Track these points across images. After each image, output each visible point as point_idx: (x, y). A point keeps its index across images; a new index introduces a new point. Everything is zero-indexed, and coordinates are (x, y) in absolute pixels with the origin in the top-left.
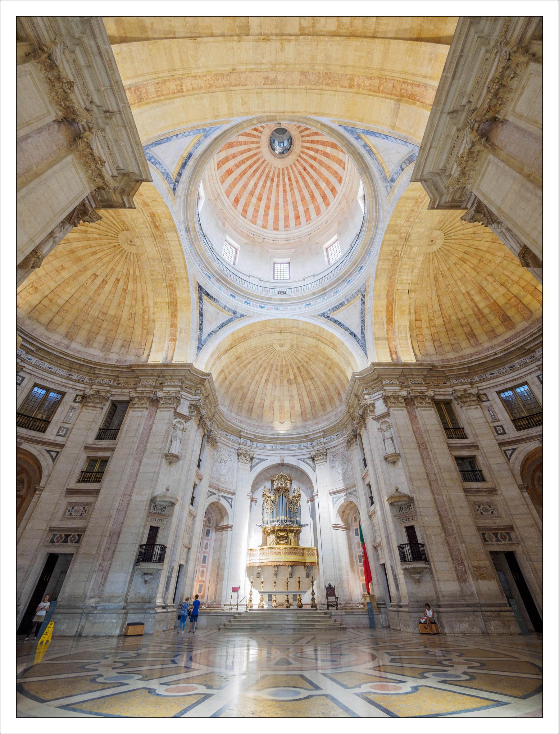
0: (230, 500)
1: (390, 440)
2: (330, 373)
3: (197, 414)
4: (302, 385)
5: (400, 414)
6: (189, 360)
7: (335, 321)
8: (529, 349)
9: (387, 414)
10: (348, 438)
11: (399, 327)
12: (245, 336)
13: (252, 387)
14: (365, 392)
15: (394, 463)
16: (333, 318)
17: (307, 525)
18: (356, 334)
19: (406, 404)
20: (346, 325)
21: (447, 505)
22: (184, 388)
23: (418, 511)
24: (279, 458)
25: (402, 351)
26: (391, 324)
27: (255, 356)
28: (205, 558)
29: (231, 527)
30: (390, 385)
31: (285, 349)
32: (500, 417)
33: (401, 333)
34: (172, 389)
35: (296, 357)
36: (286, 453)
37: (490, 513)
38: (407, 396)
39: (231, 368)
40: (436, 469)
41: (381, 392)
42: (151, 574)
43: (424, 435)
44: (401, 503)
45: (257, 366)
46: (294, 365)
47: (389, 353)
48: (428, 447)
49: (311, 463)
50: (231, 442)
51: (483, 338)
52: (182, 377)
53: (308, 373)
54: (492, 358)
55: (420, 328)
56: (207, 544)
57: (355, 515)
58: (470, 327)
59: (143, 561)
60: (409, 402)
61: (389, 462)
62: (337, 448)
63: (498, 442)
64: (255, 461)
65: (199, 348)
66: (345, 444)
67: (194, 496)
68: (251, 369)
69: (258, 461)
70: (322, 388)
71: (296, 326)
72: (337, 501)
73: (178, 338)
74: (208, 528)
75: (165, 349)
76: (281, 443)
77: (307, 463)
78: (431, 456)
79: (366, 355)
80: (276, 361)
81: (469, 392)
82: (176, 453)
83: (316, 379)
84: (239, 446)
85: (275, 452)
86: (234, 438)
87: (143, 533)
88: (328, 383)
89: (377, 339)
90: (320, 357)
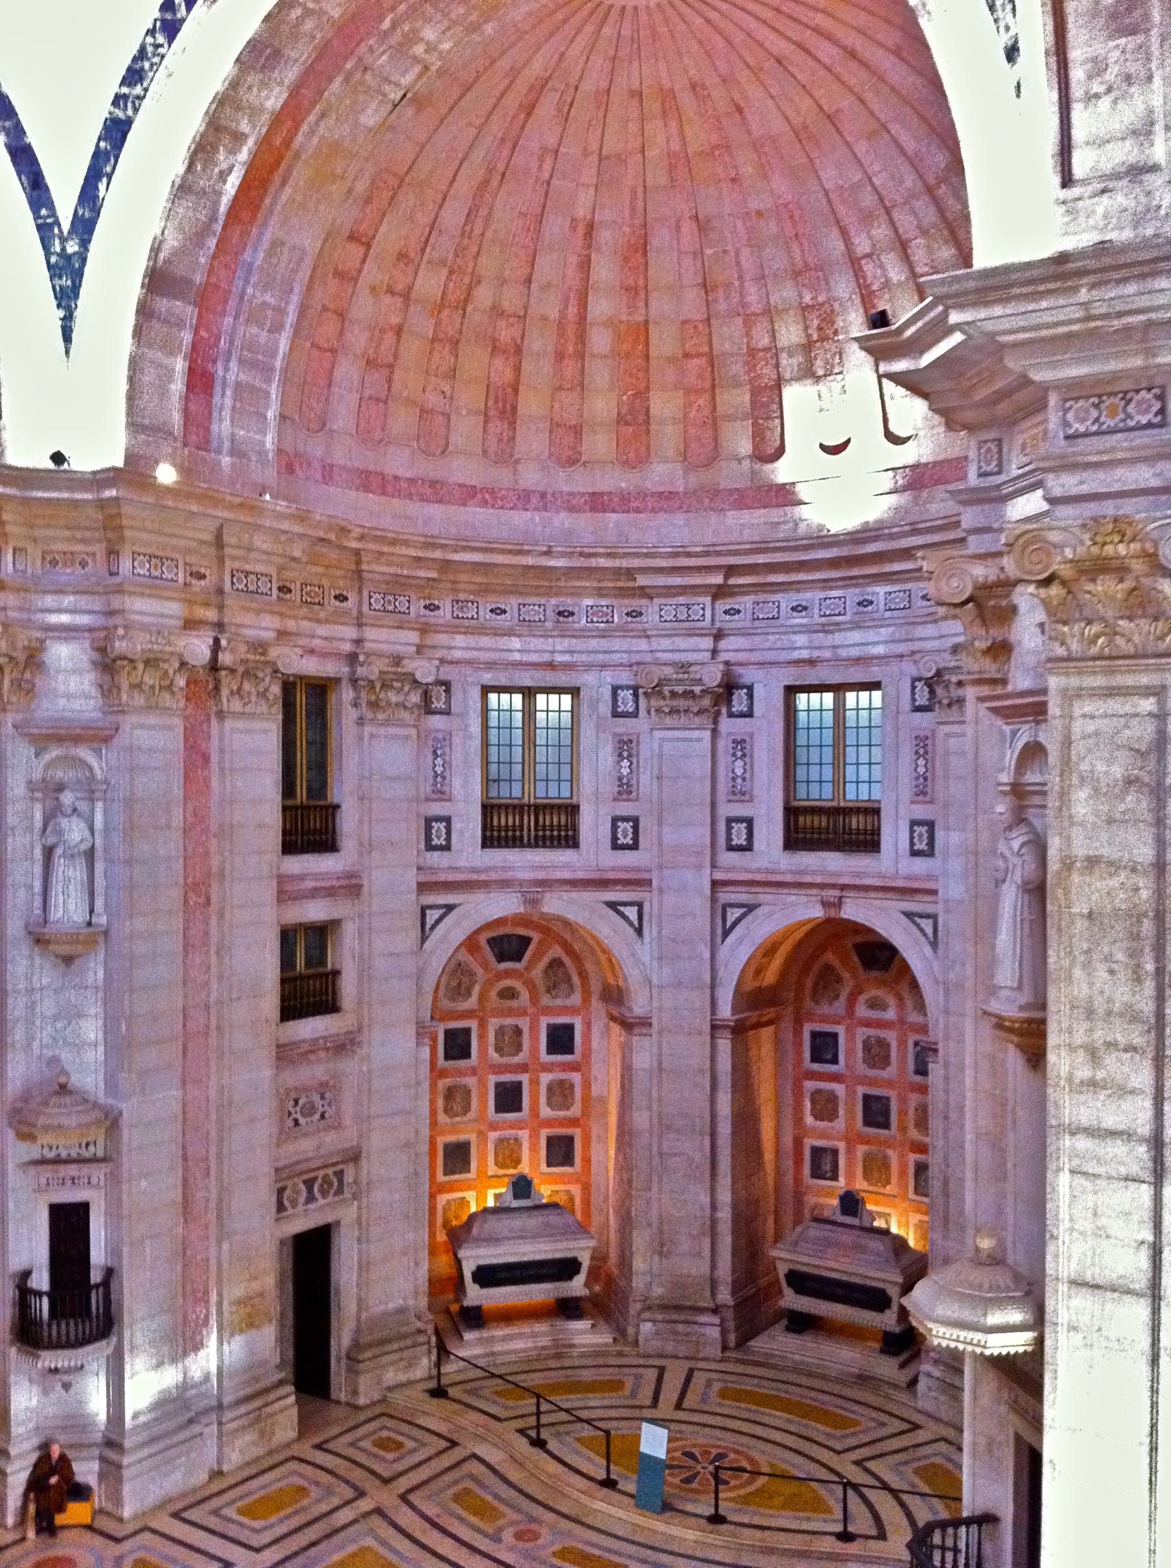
1: (81, 862)
8: (642, 588)
9: (98, 736)
32: (457, 784)
33: (266, 287)
37: (317, 1116)
41: (97, 604)
43: (213, 844)
48: (214, 899)
51: (533, 440)
54: (530, 561)
55: (347, 278)
58: (518, 369)
63: (423, 878)
81: (409, 666)
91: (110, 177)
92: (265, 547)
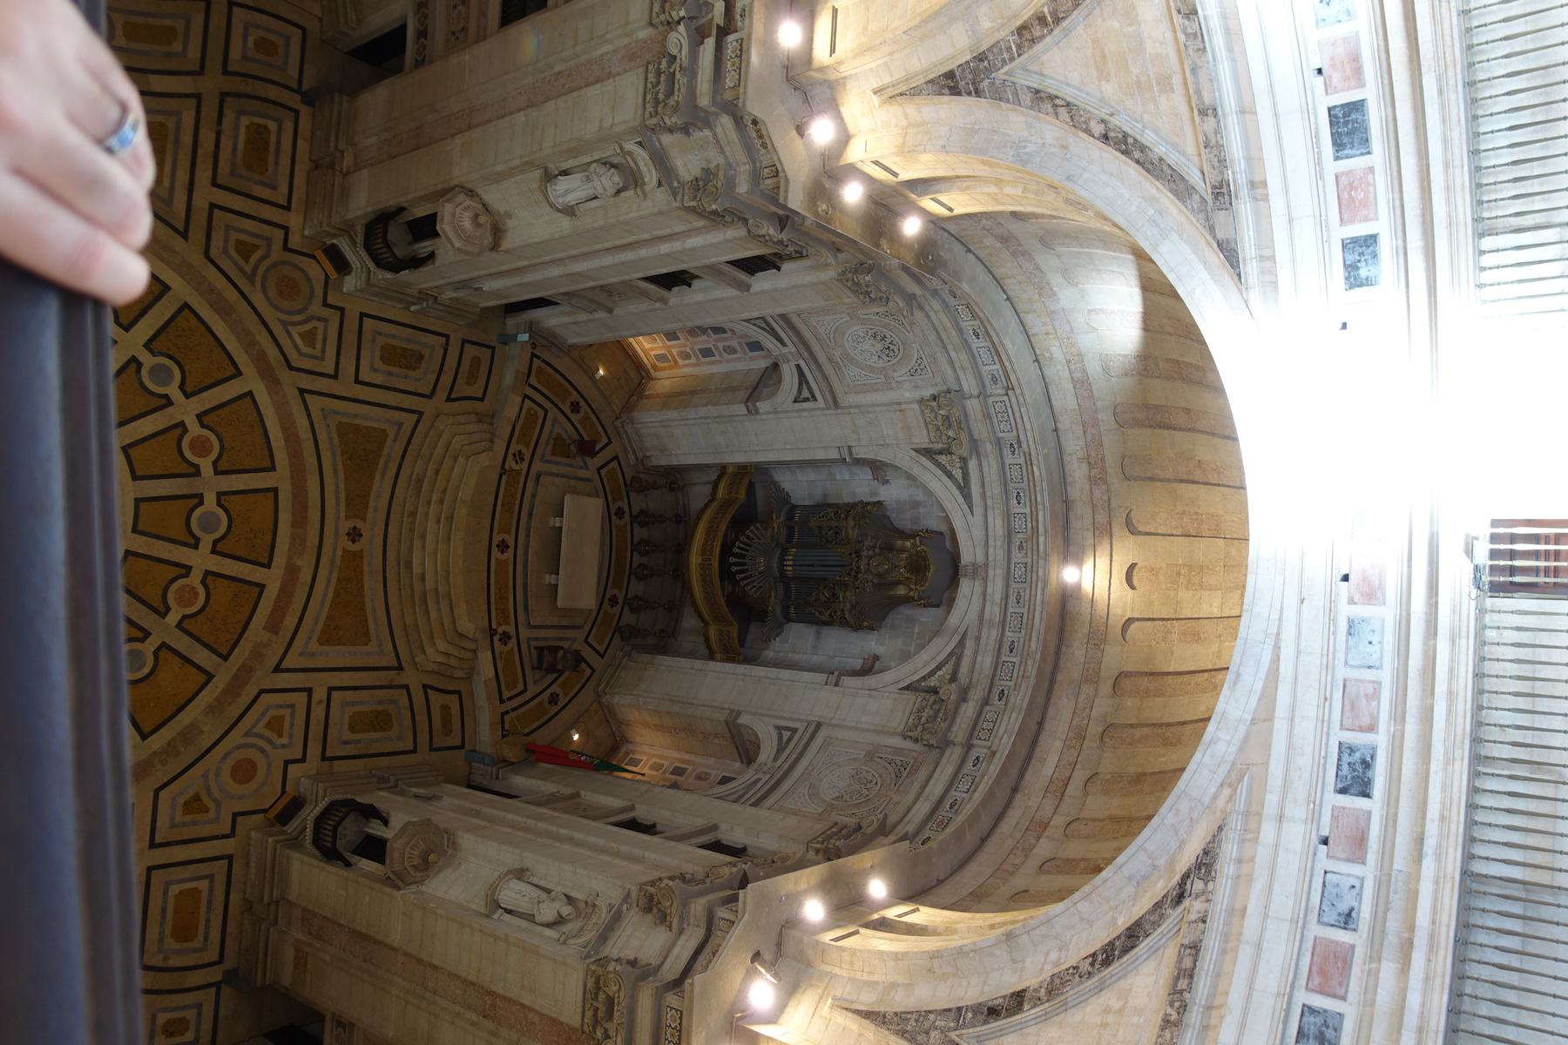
0: (806, 394)
7: (1133, 935)
16: (1156, 925)
36: (996, 587)
49: (932, 682)
56: (735, 352)
62: (916, 788)
65: (950, 83)
69: (958, 474)
72: (780, 737)
77: (939, 667)
79: (867, 1015)
84: (975, 393)
85: (999, 543)
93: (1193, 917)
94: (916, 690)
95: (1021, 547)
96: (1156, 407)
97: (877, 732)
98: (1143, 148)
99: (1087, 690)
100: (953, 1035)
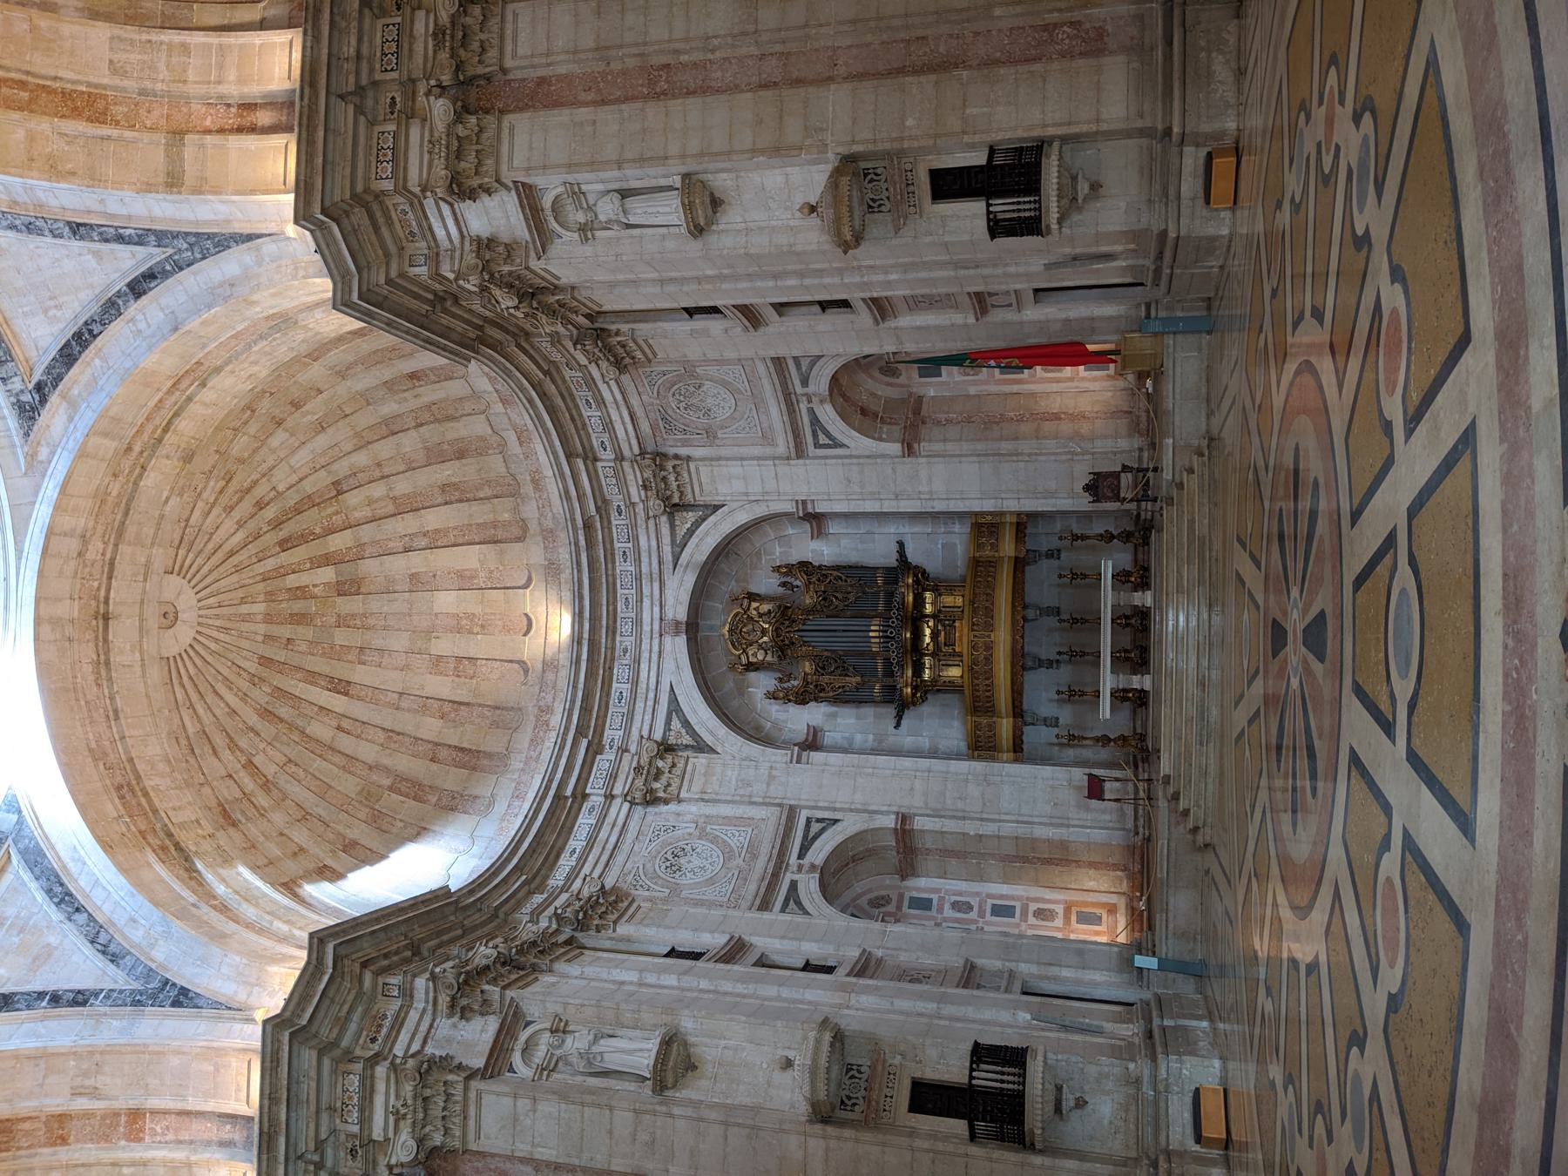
0: (815, 827)
1: (631, 203)
2: (315, 408)
3: (494, 981)
4: (366, 533)
5: (529, 143)
6: (251, 1036)
7: (68, 356)
9: (528, 196)
10: (604, 364)
11: (114, 68)
12: (119, 788)
13: (367, 752)
14: (422, 271)
15: (716, 203)
16: (49, 370)
17: (901, 544)
18: (143, 269)
19: (487, 112)
20: (95, 308)
21: (869, 38)
22: (376, 1047)
23: (887, 146)
24: (668, 640)
25: (241, 81)
26: (100, 105)
27: (219, 740)
28: (1002, 911)
29: (904, 818)
30: (398, 158)
31: (187, 602)
34: (379, 1100)
35: (232, 554)
38: (454, 101)
39: (274, 850)
40: (744, 50)
41: (429, 203)
42: (1059, 1089)
43: (616, 66)
44: (855, 204)
45: (268, 730)
46: (270, 564)
47: (251, 142)
48: (663, 60)
49: (691, 517)
50: (603, 835)
52: (326, 1062)
53: (310, 502)
56: (956, 906)
57: (877, 374)
59: (1022, 1123)
60: (478, 95)
61: (710, 223)
64: (678, 735)
65: (182, 998)
66: (625, 379)
67: (801, 964)
68: (281, 759)
70: (384, 449)
71: (74, 545)
72: (828, 435)
73: (119, 1104)
74: (906, 903)
75: (179, 1155)
76: (612, 630)
77: (691, 532)
78: (697, 56)
79: (250, 238)
80: (245, 644)
82: (653, 1045)
83: (342, 468)
84: (618, 801)
85: (645, 655)
86: (585, 821)
87: (934, 1136)
88: (365, 419)
89: (173, 182)
90: (241, 445)
91: (116, 228)
92: (354, 42)
93: (15, 379)
94: (706, 506)
95: (625, 651)
96: (464, 767)
97: (719, 459)
98: (49, 892)
99: (549, 523)
100: (170, 251)
